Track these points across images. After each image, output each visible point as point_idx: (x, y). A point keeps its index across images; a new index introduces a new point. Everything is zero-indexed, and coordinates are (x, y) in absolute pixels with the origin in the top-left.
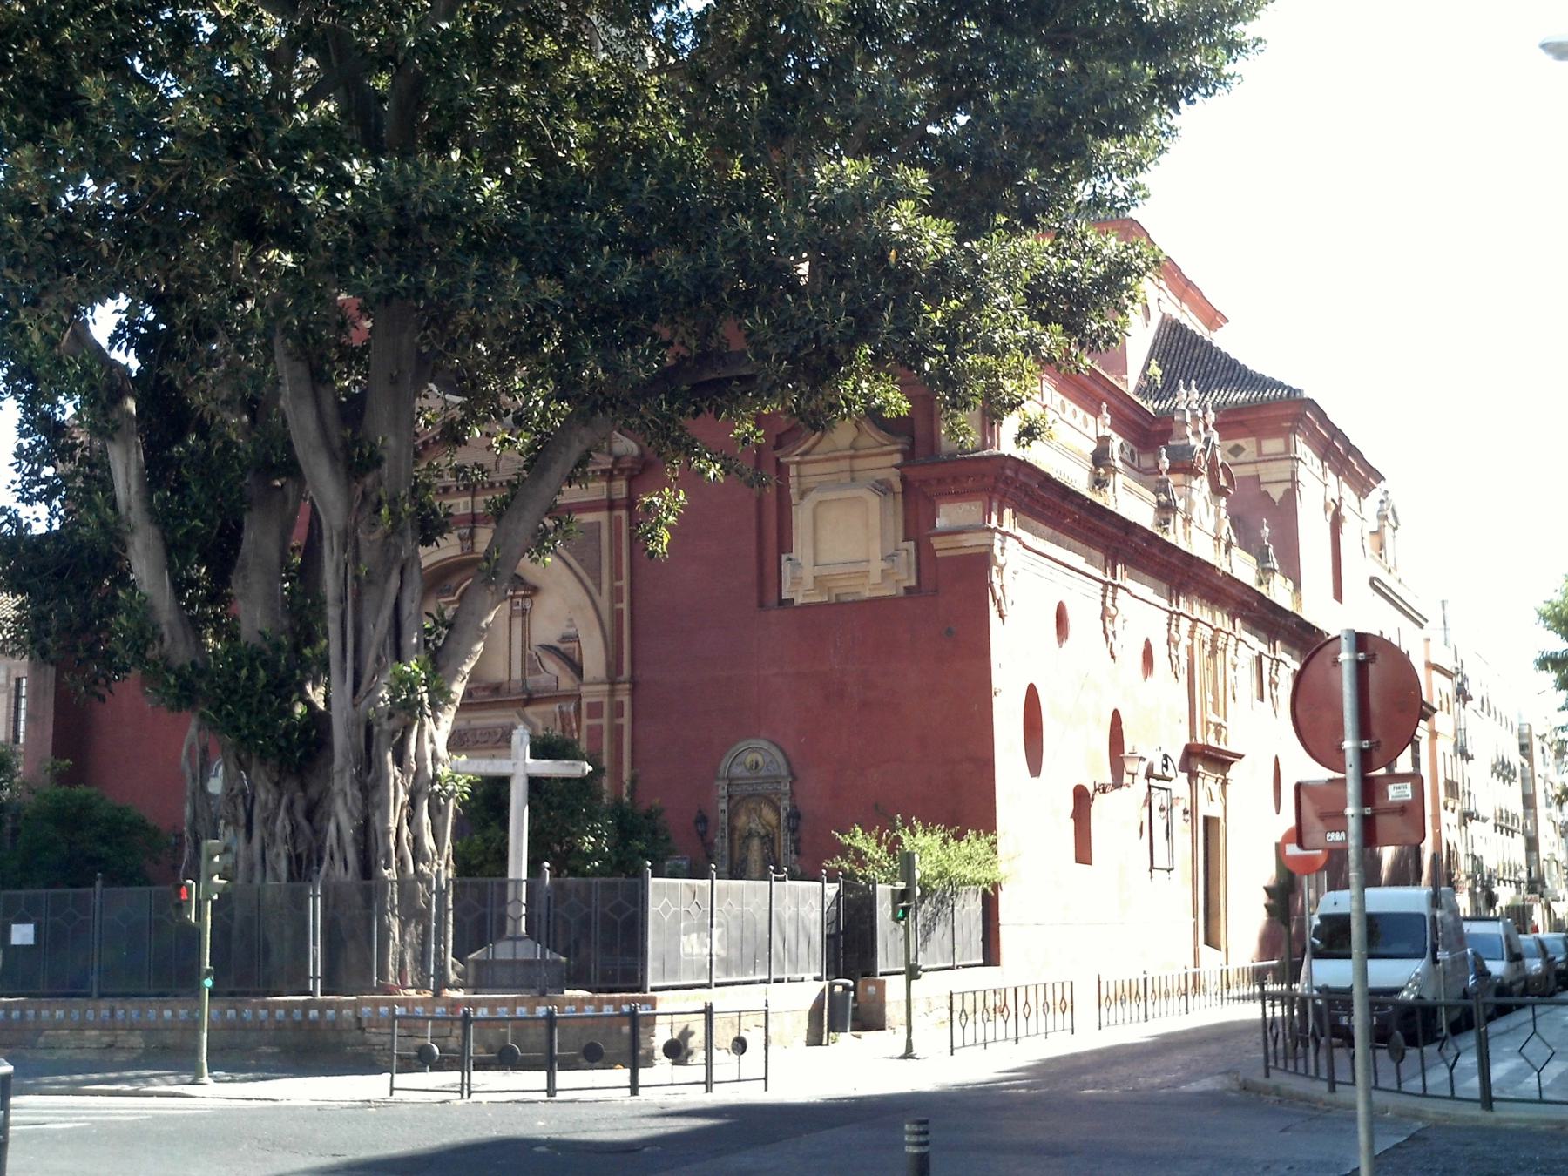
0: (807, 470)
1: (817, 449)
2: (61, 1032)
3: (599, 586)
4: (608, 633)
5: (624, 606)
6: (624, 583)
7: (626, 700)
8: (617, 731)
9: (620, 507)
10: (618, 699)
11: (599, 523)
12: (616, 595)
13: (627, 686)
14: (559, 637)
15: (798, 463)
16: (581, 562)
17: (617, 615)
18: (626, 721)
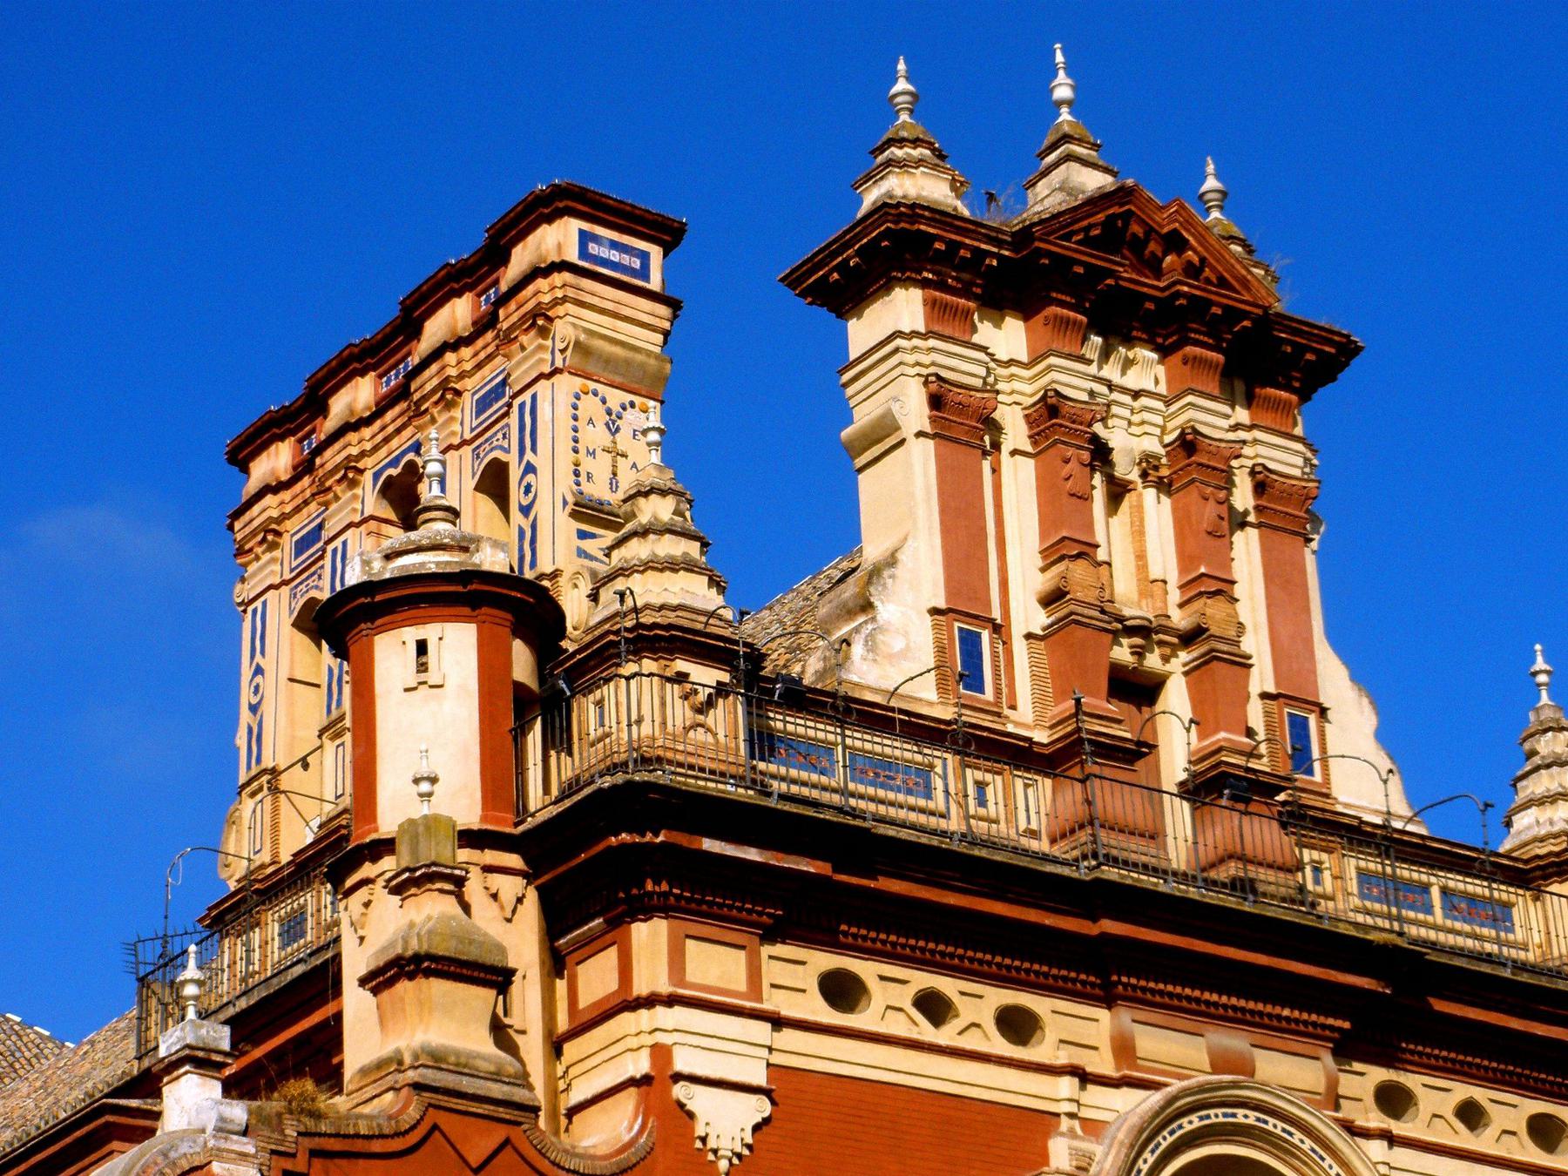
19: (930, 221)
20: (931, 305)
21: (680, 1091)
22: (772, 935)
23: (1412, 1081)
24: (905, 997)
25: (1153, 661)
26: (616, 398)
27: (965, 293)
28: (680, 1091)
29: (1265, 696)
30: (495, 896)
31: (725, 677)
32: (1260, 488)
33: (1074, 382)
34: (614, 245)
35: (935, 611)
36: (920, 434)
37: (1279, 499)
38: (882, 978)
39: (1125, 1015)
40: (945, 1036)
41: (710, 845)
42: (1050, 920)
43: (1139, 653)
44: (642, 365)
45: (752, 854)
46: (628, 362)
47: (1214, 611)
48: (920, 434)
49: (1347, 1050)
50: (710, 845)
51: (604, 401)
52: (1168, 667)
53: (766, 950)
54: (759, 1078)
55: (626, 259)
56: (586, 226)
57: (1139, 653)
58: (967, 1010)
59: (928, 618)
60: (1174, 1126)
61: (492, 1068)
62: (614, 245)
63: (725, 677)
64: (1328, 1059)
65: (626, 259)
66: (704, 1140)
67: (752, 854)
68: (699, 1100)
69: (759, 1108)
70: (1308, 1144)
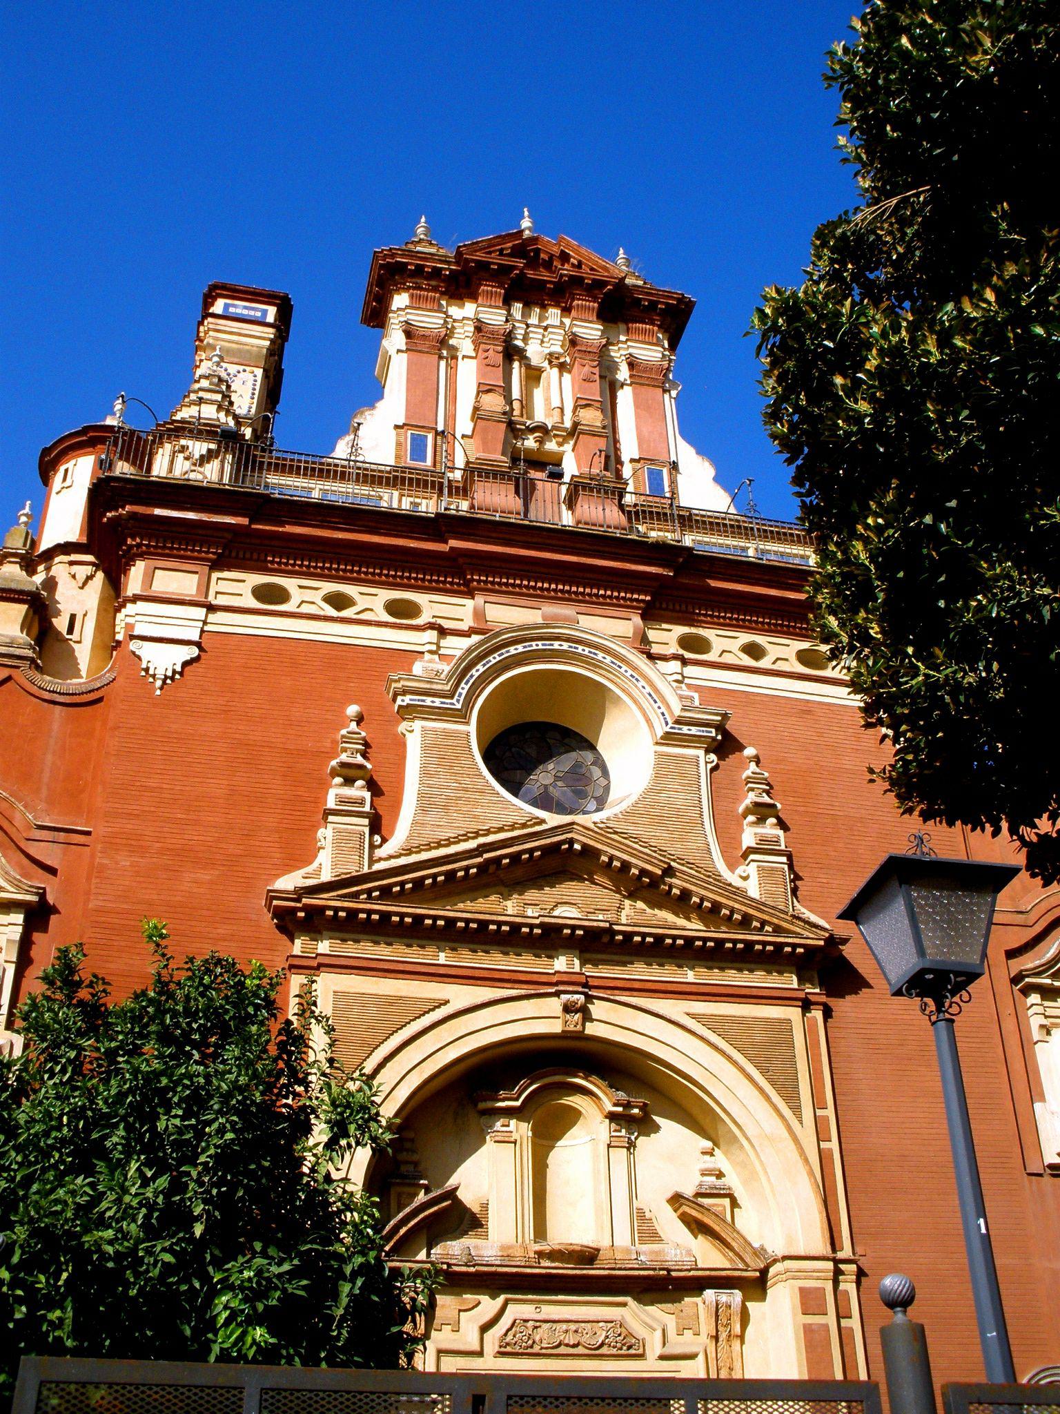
3: (797, 1110)
13: (854, 1267)
16: (764, 1072)
17: (824, 1157)
19: (402, 256)
20: (412, 296)
21: (134, 646)
22: (217, 565)
24: (317, 597)
25: (551, 446)
27: (435, 289)
28: (134, 646)
29: (632, 461)
30: (74, 577)
31: (213, 446)
32: (631, 365)
35: (397, 427)
36: (399, 351)
37: (645, 371)
38: (300, 587)
39: (480, 599)
40: (346, 613)
41: (158, 512)
42: (413, 544)
43: (541, 442)
44: (248, 351)
45: (191, 515)
46: (239, 351)
48: (399, 351)
49: (650, 615)
50: (158, 512)
51: (226, 370)
53: (215, 575)
57: (541, 442)
58: (362, 603)
59: (394, 432)
60: (503, 651)
61: (8, 641)
62: (246, 308)
63: (213, 446)
64: (637, 620)
66: (147, 670)
67: (191, 515)
68: (148, 652)
70: (609, 659)
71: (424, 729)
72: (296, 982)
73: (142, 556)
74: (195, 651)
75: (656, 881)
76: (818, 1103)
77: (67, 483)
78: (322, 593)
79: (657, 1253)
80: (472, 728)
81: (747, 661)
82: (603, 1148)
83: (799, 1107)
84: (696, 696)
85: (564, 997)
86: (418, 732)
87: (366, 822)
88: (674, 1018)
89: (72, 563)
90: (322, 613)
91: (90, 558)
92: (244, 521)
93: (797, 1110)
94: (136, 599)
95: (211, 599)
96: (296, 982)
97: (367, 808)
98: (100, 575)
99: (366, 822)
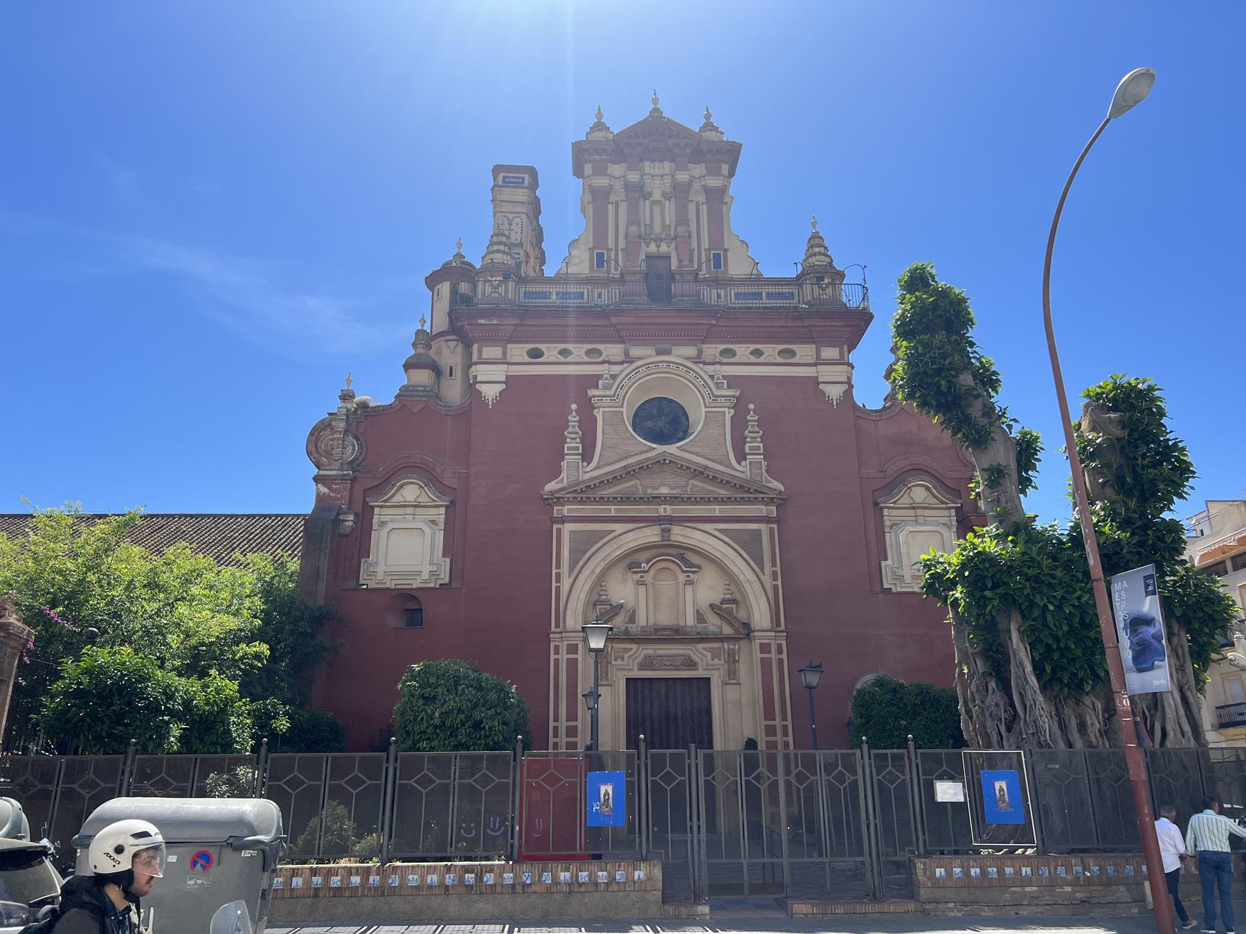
0: (894, 512)
1: (900, 502)
2: (1028, 889)
3: (762, 569)
4: (770, 597)
5: (779, 583)
6: (778, 568)
7: (784, 643)
8: (780, 662)
9: (773, 522)
10: (779, 642)
11: (760, 530)
12: (774, 575)
13: (785, 634)
14: (720, 600)
15: (889, 508)
17: (775, 588)
18: (784, 656)
23: (570, 347)
26: (511, 216)
33: (633, 177)
34: (513, 177)
36: (588, 203)
43: (658, 246)
47: (681, 229)
48: (588, 203)
52: (670, 248)
54: (504, 380)
55: (517, 180)
56: (504, 174)
57: (658, 246)
65: (517, 180)
68: (483, 388)
69: (504, 386)
71: (603, 412)
72: (555, 527)
73: (476, 342)
74: (504, 386)
75: (701, 473)
76: (774, 565)
77: (440, 297)
78: (557, 350)
79: (704, 628)
80: (624, 410)
81: (753, 359)
82: (681, 586)
83: (763, 568)
84: (725, 381)
85: (663, 526)
86: (601, 414)
87: (580, 457)
88: (709, 531)
89: (447, 341)
90: (558, 361)
91: (454, 337)
92: (519, 322)
93: (762, 569)
94: (476, 364)
95: (509, 359)
96: (555, 527)
97: (580, 451)
98: (460, 344)
99: (580, 457)
